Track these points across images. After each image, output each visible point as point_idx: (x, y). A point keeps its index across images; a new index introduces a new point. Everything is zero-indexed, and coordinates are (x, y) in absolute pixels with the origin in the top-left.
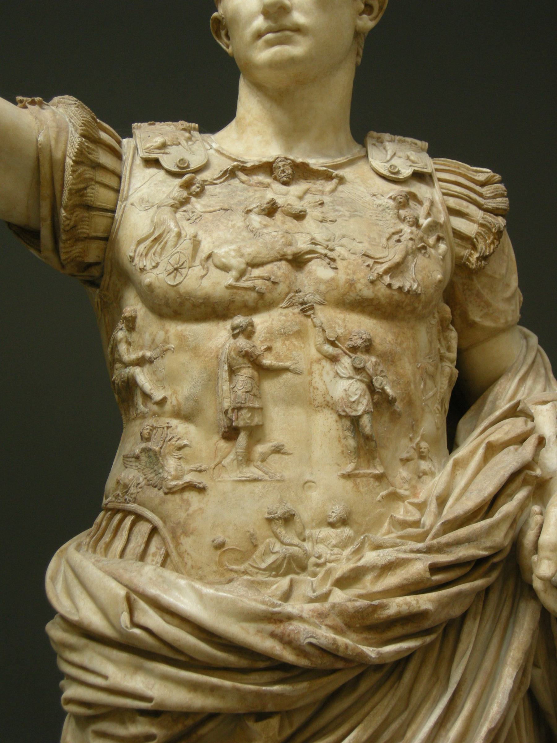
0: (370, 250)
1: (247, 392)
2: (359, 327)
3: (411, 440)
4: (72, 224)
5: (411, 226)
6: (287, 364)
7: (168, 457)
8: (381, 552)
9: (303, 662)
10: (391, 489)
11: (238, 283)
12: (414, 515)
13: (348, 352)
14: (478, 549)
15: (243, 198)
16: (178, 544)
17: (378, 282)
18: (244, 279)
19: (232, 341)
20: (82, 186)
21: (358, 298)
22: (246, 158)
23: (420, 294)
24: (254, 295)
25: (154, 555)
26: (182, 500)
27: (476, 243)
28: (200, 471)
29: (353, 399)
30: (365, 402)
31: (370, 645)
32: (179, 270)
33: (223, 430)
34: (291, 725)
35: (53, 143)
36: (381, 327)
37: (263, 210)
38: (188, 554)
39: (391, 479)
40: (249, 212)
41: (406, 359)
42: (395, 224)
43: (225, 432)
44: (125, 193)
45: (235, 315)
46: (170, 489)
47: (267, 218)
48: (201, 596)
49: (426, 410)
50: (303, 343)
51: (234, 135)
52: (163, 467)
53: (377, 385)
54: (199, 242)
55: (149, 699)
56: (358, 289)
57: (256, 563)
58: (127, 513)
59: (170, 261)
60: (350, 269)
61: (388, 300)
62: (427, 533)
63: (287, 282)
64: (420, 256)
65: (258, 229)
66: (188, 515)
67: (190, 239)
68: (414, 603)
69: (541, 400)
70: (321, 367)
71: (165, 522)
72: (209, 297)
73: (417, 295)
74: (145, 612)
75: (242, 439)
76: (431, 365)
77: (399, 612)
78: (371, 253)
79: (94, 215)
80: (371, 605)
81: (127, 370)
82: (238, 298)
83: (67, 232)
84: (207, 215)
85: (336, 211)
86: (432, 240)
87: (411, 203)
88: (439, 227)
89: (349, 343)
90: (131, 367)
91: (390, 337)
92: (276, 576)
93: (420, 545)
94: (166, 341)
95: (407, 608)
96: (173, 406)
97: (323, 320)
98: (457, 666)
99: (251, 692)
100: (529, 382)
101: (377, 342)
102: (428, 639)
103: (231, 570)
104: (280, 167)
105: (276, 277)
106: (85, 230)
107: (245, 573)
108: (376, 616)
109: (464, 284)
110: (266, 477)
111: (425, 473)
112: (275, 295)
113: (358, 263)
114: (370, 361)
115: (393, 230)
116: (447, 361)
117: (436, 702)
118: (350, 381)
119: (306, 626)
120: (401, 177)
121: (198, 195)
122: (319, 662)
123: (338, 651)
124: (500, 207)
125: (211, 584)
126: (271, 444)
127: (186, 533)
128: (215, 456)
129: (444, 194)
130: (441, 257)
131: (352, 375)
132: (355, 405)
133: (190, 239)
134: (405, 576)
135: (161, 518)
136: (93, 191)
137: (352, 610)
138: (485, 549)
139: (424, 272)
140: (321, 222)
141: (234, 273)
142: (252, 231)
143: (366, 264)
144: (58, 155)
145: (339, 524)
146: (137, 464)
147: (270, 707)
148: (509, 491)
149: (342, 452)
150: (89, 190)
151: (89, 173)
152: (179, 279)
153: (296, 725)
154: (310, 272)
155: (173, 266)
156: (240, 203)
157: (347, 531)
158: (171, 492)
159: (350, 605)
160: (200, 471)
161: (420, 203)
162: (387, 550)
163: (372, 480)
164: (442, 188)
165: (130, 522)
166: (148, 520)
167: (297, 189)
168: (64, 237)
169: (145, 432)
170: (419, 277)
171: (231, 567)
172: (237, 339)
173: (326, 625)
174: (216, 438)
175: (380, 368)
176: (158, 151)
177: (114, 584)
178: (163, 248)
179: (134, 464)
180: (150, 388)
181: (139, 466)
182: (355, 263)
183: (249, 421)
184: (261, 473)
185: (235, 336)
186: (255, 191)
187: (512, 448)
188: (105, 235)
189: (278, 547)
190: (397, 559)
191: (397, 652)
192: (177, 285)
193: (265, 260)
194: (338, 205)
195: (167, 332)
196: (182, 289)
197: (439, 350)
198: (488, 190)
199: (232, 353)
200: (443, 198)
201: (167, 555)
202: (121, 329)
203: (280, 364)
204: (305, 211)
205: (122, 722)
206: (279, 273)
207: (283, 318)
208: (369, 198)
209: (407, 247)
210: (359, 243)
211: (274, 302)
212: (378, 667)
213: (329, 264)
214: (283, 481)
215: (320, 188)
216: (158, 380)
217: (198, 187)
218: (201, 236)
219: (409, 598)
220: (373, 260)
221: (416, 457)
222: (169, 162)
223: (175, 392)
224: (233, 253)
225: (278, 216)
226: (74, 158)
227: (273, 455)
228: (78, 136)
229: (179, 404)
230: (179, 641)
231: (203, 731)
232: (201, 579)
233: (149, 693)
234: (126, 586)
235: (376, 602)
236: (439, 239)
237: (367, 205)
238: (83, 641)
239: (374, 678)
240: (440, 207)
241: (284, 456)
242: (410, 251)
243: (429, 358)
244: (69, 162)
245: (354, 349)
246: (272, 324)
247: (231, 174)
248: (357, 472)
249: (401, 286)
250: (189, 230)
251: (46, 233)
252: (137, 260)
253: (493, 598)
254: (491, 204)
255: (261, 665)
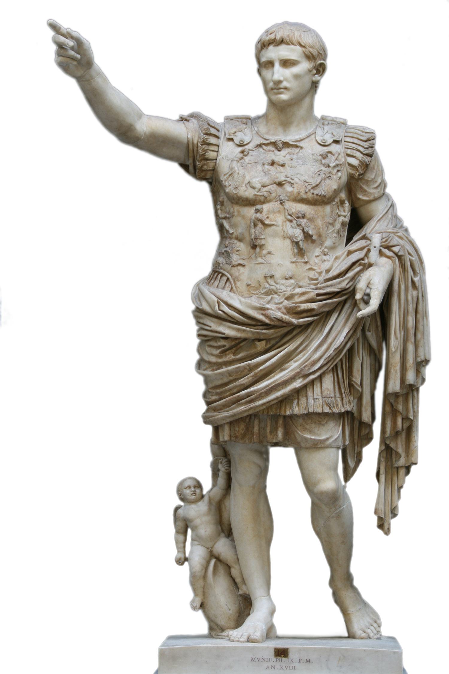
0: (308, 179)
1: (259, 233)
2: (301, 209)
3: (320, 249)
4: (201, 166)
5: (326, 167)
6: (274, 223)
7: (233, 254)
8: (301, 289)
9: (272, 323)
10: (310, 266)
11: (258, 193)
12: (317, 276)
13: (296, 219)
14: (336, 289)
15: (263, 157)
16: (235, 284)
17: (309, 192)
18: (260, 191)
19: (255, 215)
20: (204, 152)
21: (301, 198)
22: (267, 137)
23: (325, 196)
24: (263, 198)
25: (228, 287)
26: (237, 269)
27: (358, 168)
28: (244, 259)
29: (296, 236)
30: (301, 236)
31: (296, 319)
32: (238, 188)
33: (251, 245)
34: (270, 344)
35: (193, 137)
36: (310, 208)
37: (269, 164)
38: (239, 287)
39: (311, 263)
40: (264, 164)
41: (319, 220)
42: (320, 167)
43: (252, 246)
44: (220, 153)
45: (257, 205)
46: (233, 265)
47: (270, 166)
48: (240, 302)
49: (328, 237)
50: (280, 215)
51: (265, 123)
52: (231, 257)
53: (305, 230)
54: (245, 177)
55: (224, 334)
56: (301, 195)
57: (260, 291)
58: (219, 273)
59: (235, 184)
60: (298, 187)
61: (312, 199)
62: (319, 283)
63: (276, 193)
64: (328, 180)
65: (267, 171)
66: (239, 274)
67: (242, 176)
68: (310, 306)
69: (379, 232)
70: (286, 224)
71: (231, 276)
72: (248, 198)
73: (324, 196)
74: (223, 306)
75: (258, 249)
76: (331, 220)
77: (304, 309)
78: (307, 181)
79: (209, 162)
80: (295, 306)
81: (221, 221)
82: (258, 199)
83: (198, 169)
84: (249, 166)
85: (298, 162)
86: (335, 171)
87: (329, 155)
88: (339, 166)
89: (297, 215)
90: (222, 220)
91: (313, 212)
92: (266, 296)
93: (313, 287)
94: (234, 212)
95: (307, 307)
96: (236, 236)
97: (288, 206)
98: (328, 327)
99: (256, 332)
100: (381, 222)
101: (307, 215)
102: (316, 318)
103: (252, 293)
104: (277, 144)
105: (272, 191)
106: (205, 168)
107: (257, 294)
108: (297, 309)
109: (355, 183)
110: (265, 262)
111: (325, 261)
112: (271, 197)
113: (302, 185)
114: (303, 222)
115: (318, 170)
116: (342, 216)
117: (319, 339)
118: (296, 229)
119: (273, 312)
120: (327, 144)
121: (246, 156)
122: (277, 323)
123: (283, 320)
124: (369, 153)
125: (245, 297)
126: (268, 251)
127: (238, 280)
128: (249, 254)
129: (346, 148)
130: (338, 178)
131: (296, 227)
132: (297, 238)
133: (242, 176)
134: (309, 297)
135: (230, 275)
136: (208, 153)
137: (289, 307)
138: (338, 289)
139: (328, 187)
140: (291, 167)
141: (257, 190)
142: (264, 172)
143: (305, 185)
144: (195, 142)
145: (289, 279)
146: (223, 256)
147: (262, 337)
148: (353, 268)
149: (292, 254)
150: (206, 154)
151: (205, 147)
152: (237, 191)
153: (271, 344)
154: (284, 189)
155: (236, 186)
156: (262, 159)
157: (292, 281)
158: (233, 266)
159: (288, 306)
160: (244, 259)
161: (334, 155)
162: (303, 288)
163: (303, 264)
164: (345, 145)
165: (220, 276)
166: (226, 276)
167: (284, 152)
168: (197, 171)
169: (226, 244)
170: (326, 189)
171: (252, 292)
172: (257, 214)
173: (280, 312)
174: (250, 248)
175: (308, 224)
176: (233, 135)
177: (213, 297)
178: (233, 178)
179: (222, 255)
180: (228, 228)
181: (224, 256)
182: (301, 185)
183: (259, 243)
184: (263, 261)
185: (256, 213)
186: (268, 154)
187: (357, 252)
188: (213, 169)
189: (267, 286)
190: (306, 291)
191: (305, 322)
192: (237, 193)
193: (268, 184)
194: (298, 159)
195: (234, 209)
196: (238, 195)
197: (338, 213)
198: (367, 144)
199: (255, 219)
200: (345, 150)
201: (232, 288)
202: (219, 205)
203: (272, 223)
204: (285, 164)
205: (216, 342)
206: (273, 189)
207: (274, 206)
208: (311, 156)
209: (322, 177)
210: (304, 176)
211: (270, 200)
212: (299, 326)
213: (291, 185)
214: (271, 264)
215: (293, 152)
216: (231, 226)
217: (247, 153)
218: (246, 174)
219: (308, 304)
220: (308, 183)
221: (322, 254)
222: (237, 140)
223: (236, 231)
224: (257, 182)
225: (275, 165)
226: (201, 143)
227: (268, 255)
228: (203, 135)
229: (237, 235)
230: (233, 315)
231: (241, 345)
232: (242, 296)
233: (224, 332)
234: (217, 297)
235: (297, 305)
236: (338, 171)
237: (310, 159)
238: (204, 316)
239: (298, 330)
240: (342, 154)
241: (272, 255)
242: (323, 179)
243: (331, 218)
244: (199, 145)
245: (298, 218)
246: (269, 208)
247: (260, 146)
248: (297, 261)
249: (317, 193)
250: (242, 172)
251: (191, 168)
252: (223, 182)
253: (347, 305)
254: (366, 151)
255: (259, 324)
